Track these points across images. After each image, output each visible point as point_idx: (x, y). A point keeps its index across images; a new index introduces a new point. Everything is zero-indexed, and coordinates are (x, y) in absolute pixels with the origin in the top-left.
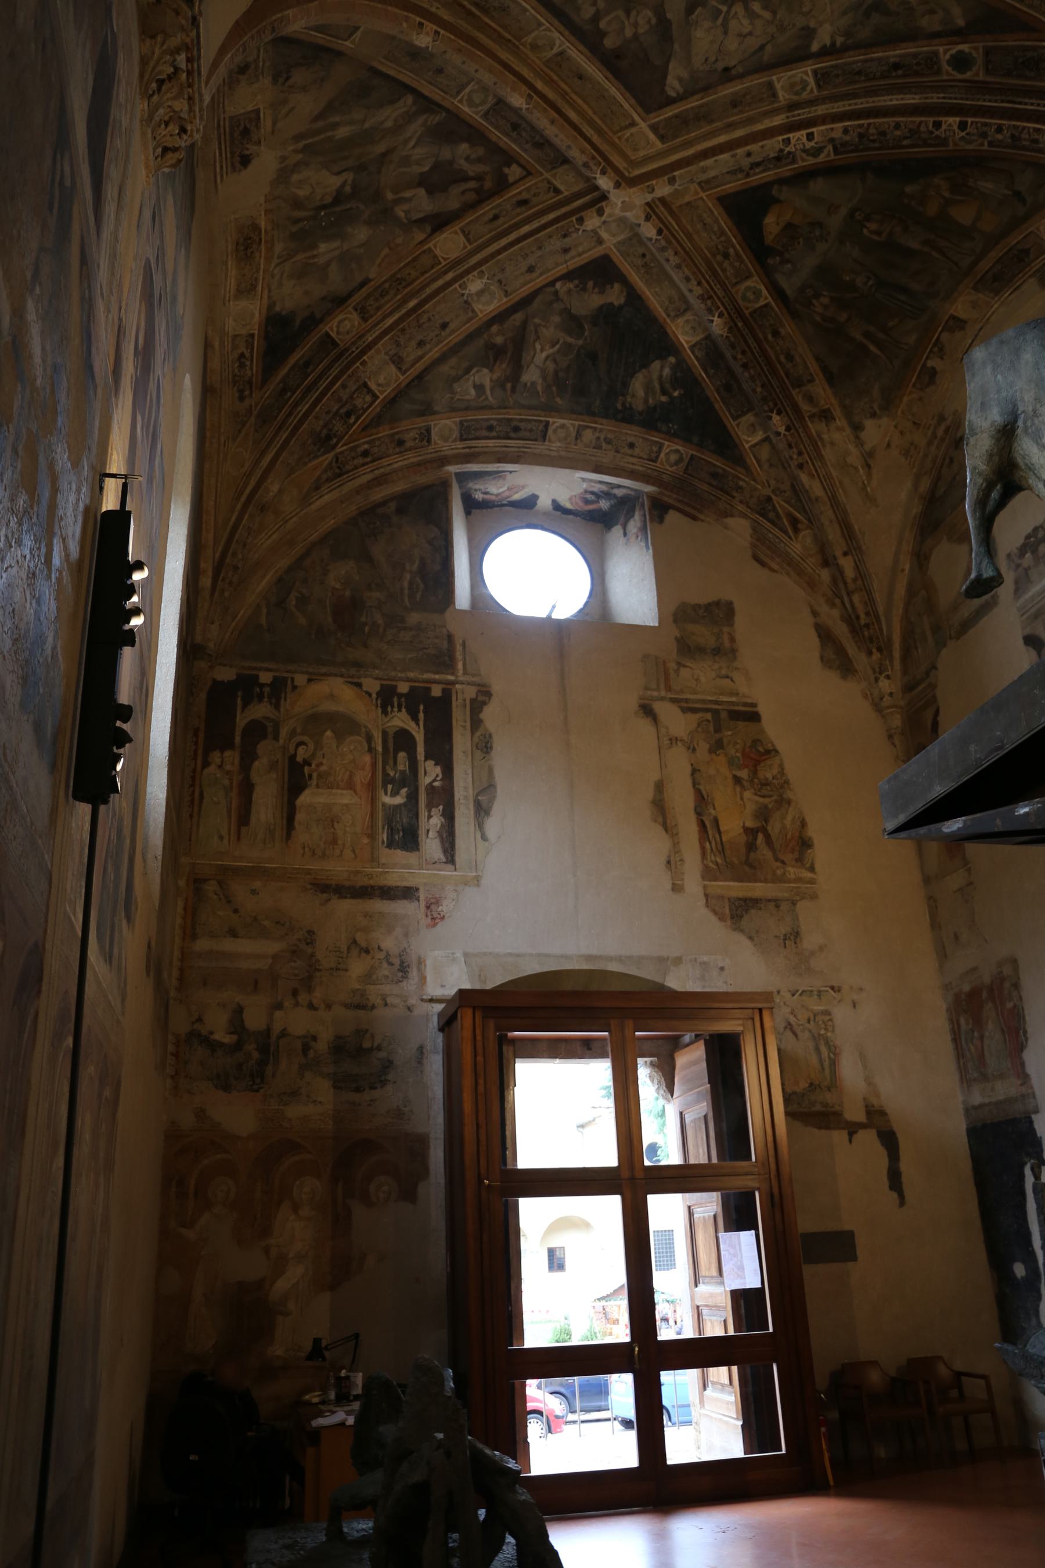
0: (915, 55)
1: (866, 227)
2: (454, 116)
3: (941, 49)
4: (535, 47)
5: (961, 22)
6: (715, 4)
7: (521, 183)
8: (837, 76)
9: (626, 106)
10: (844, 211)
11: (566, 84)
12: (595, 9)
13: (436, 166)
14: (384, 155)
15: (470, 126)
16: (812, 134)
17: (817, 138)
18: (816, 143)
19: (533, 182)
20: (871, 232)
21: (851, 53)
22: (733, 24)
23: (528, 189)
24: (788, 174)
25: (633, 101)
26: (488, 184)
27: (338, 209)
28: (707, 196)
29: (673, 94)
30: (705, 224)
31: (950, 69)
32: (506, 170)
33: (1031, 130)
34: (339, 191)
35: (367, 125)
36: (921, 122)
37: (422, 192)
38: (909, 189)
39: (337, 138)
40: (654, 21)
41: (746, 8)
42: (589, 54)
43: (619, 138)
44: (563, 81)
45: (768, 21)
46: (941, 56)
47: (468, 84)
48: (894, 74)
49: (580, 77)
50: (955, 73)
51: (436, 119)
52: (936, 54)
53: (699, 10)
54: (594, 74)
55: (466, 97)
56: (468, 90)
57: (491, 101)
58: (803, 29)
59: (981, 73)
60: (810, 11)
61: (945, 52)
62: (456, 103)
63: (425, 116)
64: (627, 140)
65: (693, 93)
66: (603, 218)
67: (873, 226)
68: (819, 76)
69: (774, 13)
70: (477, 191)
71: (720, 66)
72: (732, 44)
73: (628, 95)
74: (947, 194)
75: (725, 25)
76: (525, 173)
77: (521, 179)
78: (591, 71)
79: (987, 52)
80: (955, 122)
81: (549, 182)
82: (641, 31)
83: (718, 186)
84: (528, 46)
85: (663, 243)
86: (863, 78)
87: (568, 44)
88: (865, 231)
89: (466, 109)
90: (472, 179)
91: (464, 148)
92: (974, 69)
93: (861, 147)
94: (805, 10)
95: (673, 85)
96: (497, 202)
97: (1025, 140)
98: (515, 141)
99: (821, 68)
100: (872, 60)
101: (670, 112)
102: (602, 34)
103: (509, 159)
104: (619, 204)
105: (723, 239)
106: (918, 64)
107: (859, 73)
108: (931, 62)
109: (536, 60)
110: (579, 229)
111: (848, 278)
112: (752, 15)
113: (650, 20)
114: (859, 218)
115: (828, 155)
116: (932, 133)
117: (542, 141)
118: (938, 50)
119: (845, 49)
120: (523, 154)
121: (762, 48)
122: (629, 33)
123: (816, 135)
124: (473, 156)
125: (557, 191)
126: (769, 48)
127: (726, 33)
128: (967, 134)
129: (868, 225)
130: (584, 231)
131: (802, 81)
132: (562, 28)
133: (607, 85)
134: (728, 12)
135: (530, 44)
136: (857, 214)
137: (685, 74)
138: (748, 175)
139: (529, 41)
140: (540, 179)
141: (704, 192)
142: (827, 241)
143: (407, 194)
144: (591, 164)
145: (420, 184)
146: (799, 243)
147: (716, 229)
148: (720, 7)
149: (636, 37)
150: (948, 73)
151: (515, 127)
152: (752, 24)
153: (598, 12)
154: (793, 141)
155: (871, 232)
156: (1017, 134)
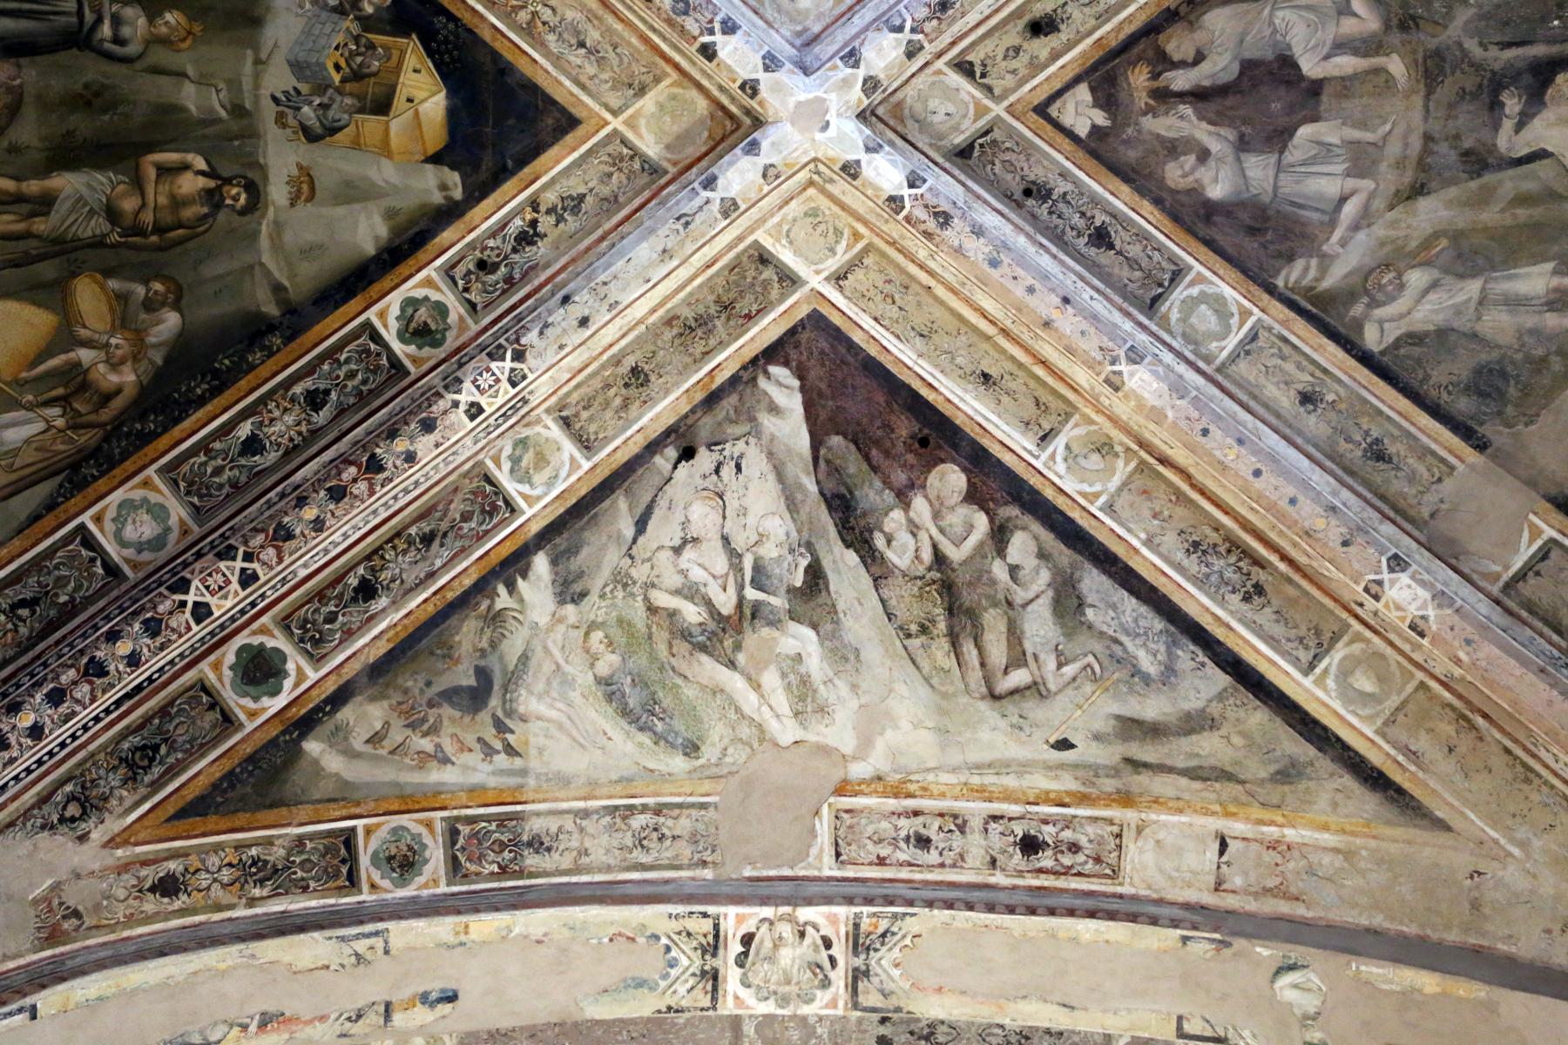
0: (349, 634)
1: (202, 173)
2: (1258, 277)
3: (313, 676)
4: (1104, 448)
5: (312, 746)
6: (773, 600)
7: (1058, 86)
8: (466, 517)
9: (867, 322)
10: (277, 192)
11: (1013, 359)
12: (1009, 560)
13: (1278, 138)
14: (1418, 190)
15: (1209, 244)
16: (472, 418)
17: (460, 415)
18: (456, 404)
19: (1028, 87)
20: (186, 167)
21: (468, 582)
22: (721, 564)
23: (1036, 67)
24: (447, 235)
25: (857, 337)
26: (1139, 79)
27: (1539, 50)
28: (607, 123)
29: (773, 369)
30: (582, 45)
31: (270, 643)
32: (1100, 118)
33: (78, 708)
34: (1536, 97)
35: (1474, 287)
36: (280, 560)
37: (1310, 67)
38: (171, 321)
39: (1550, 266)
40: (879, 541)
41: (709, 604)
42: (985, 442)
43: (856, 236)
44: (1021, 365)
45: (653, 585)
46: (303, 663)
47: (1234, 357)
48: (361, 571)
49: (986, 377)
50: (256, 640)
51: (1292, 275)
52: (317, 660)
53: (798, 582)
54: (959, 392)
55: (1235, 321)
56: (1232, 342)
57: (1172, 306)
58: (583, 595)
59: (212, 676)
60: (587, 634)
61: (301, 676)
62: (1255, 310)
63: (1327, 284)
64: (838, 233)
65: (734, 381)
66: (861, 73)
67: (190, 184)
68: (500, 503)
69: (652, 610)
70: (1163, 62)
71: (705, 460)
72: (703, 517)
73: (873, 351)
74: (85, 355)
75: (734, 556)
76: (1053, 111)
77: (1059, 93)
78: (968, 398)
79: (228, 721)
80: (219, 607)
81: (989, 89)
82: (897, 515)
83: (590, 152)
84: (1118, 448)
85: (691, 25)
86: (413, 530)
87: (1038, 464)
88: (200, 164)
89: (1228, 292)
90: (1182, 96)
91: (1216, 192)
92: (227, 674)
93: (326, 367)
94: (598, 635)
95: (782, 387)
96: (1107, 27)
97: (75, 683)
98: (1095, 201)
99: (504, 523)
100: (421, 584)
101: (766, 329)
102: (973, 496)
103: (1096, 147)
104: (831, 117)
105: (523, 16)
106: (331, 618)
107: (428, 539)
108: (314, 642)
109: (1094, 416)
110: (913, 30)
111: (169, 17)
112: (691, 592)
113: (889, 542)
114: (234, 191)
115: (382, 315)
116: (248, 557)
117: (1030, 202)
118: (316, 670)
119: (482, 587)
120: (1068, 165)
121: (641, 525)
122: (920, 505)
123: (465, 419)
124: (1190, 160)
125: (964, 68)
126: (629, 532)
127: (726, 540)
128: (183, 604)
129: (202, 182)
130: (900, 29)
131: (525, 478)
132: (1061, 502)
133: (925, 368)
134: (740, 588)
135: (1117, 455)
136: (243, 198)
137: (767, 422)
138: (534, 204)
139: (1120, 463)
140: (1012, 99)
141: (615, 132)
142: (275, 99)
143: (1346, 64)
144: (931, 225)
145: (1316, 88)
146: (337, 67)
147: (551, 38)
148: (760, 596)
149: (903, 497)
150: (263, 631)
151: (1101, 238)
152: (684, 573)
153: (1001, 552)
154: (505, 385)
155: (186, 167)
156: (98, 681)
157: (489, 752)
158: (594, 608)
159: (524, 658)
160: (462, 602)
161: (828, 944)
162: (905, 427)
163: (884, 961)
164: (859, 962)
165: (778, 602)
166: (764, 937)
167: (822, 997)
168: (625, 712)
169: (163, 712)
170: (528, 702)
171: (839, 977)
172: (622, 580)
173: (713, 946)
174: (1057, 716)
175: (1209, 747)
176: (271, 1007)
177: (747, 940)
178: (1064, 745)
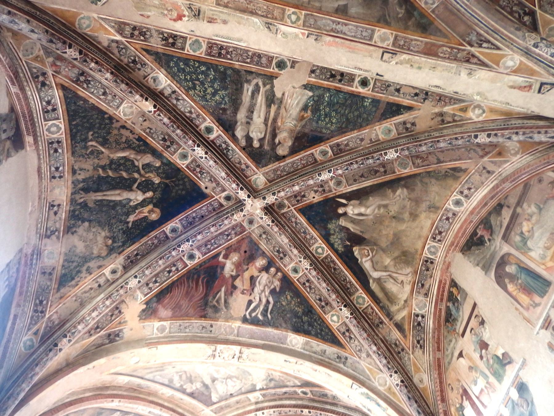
65: (223, 400)
69: (241, 381)
102: (185, 389)
112: (234, 382)
157: (272, 374)
158: (251, 383)
159: (263, 381)
160: (271, 388)
161: (219, 356)
162: (195, 395)
163: (210, 352)
164: (214, 353)
165: (220, 379)
166: (231, 357)
167: (221, 348)
168: (248, 373)
169: (319, 397)
170: (264, 377)
171: (218, 351)
172: (245, 384)
173: (239, 358)
174: (175, 370)
175: (149, 371)
176: (314, 372)
177: (233, 358)
178: (174, 367)
